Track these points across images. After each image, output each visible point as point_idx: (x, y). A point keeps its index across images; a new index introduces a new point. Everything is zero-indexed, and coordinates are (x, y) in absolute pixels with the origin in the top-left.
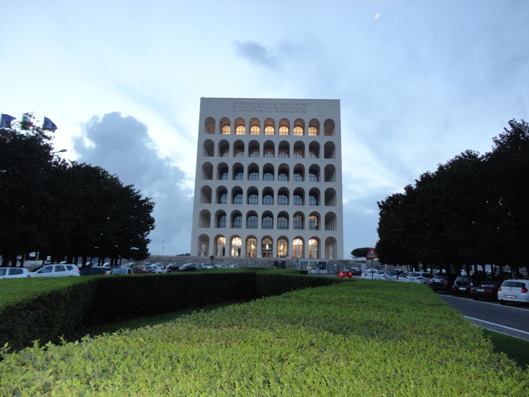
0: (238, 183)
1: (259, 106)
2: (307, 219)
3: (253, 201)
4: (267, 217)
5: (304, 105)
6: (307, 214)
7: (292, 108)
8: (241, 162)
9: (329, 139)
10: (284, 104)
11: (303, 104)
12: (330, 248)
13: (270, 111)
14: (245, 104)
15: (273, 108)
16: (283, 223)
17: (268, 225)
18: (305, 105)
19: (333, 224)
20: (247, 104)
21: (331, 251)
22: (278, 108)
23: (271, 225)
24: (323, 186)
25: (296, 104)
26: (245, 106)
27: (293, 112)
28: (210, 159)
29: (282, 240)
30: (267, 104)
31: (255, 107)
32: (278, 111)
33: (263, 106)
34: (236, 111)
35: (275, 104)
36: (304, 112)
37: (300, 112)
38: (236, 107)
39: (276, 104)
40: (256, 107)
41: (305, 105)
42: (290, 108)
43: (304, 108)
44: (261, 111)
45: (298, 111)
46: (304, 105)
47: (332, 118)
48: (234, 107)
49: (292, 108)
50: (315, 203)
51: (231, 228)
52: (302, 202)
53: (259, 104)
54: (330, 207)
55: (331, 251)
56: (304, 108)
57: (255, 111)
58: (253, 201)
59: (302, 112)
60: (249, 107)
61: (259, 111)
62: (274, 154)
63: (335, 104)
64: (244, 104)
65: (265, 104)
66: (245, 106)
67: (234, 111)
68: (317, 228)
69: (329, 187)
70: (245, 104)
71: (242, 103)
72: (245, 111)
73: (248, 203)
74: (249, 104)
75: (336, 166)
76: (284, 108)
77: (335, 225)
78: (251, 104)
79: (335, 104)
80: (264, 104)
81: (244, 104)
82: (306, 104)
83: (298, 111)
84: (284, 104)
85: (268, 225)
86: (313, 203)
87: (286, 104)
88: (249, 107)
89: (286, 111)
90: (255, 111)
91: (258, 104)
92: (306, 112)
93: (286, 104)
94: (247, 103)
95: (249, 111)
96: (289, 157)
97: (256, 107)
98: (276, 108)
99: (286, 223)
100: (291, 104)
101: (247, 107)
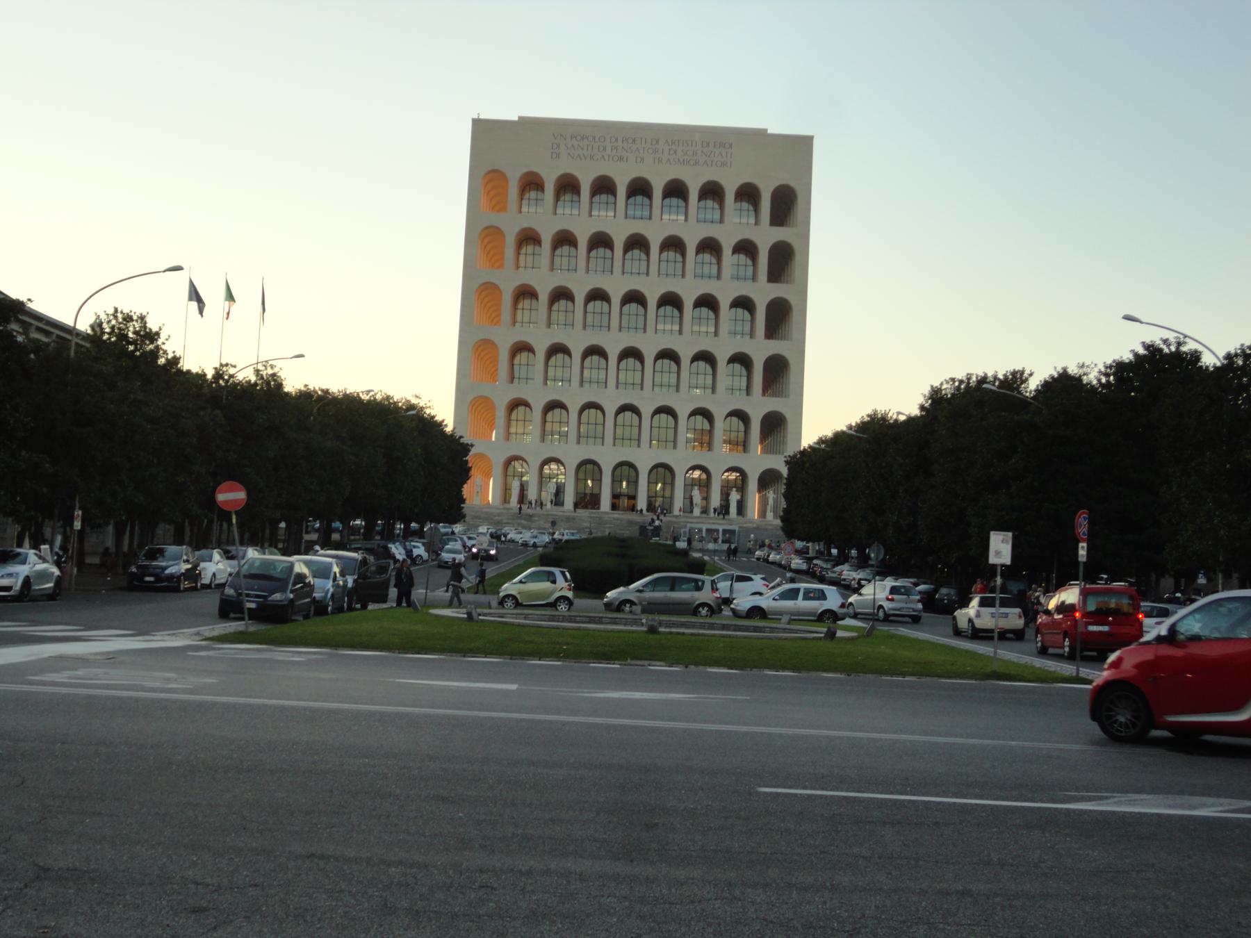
0: (560, 336)
1: (615, 144)
2: (719, 424)
3: (594, 376)
4: (626, 413)
5: (724, 147)
6: (719, 413)
7: (695, 153)
8: (569, 286)
9: (780, 234)
10: (677, 143)
11: (722, 145)
12: (768, 495)
13: (642, 160)
14: (583, 138)
15: (650, 151)
16: (663, 431)
17: (627, 435)
18: (727, 146)
19: (782, 434)
20: (585, 140)
21: (771, 502)
22: (660, 151)
23: (635, 436)
24: (760, 350)
25: (705, 145)
26: (581, 144)
27: (697, 163)
28: (496, 277)
29: (661, 470)
30: (634, 141)
31: (605, 149)
32: (660, 161)
33: (625, 145)
34: (558, 155)
35: (654, 142)
36: (724, 164)
37: (714, 163)
38: (558, 146)
39: (658, 142)
40: (609, 148)
41: (727, 146)
42: (690, 153)
43: (724, 154)
44: (621, 159)
45: (710, 163)
46: (724, 147)
47: (792, 184)
48: (555, 146)
49: (695, 153)
50: (744, 384)
51: (541, 442)
52: (711, 382)
53: (616, 140)
54: (773, 399)
55: (771, 502)
56: (724, 154)
57: (606, 158)
58: (594, 376)
59: (719, 164)
60: (590, 148)
61: (616, 158)
62: (648, 254)
63: (800, 147)
64: (579, 138)
65: (630, 141)
66: (581, 144)
67: (554, 156)
68: (745, 445)
69: (776, 352)
70: (583, 138)
71: (573, 137)
72: (583, 158)
73: (582, 382)
74: (591, 139)
75: (793, 299)
76: (675, 152)
77: (785, 440)
78: (597, 139)
79: (800, 147)
80: (627, 139)
81: (579, 138)
82: (731, 145)
83: (710, 163)
84: (677, 143)
85: (627, 435)
86: (736, 384)
87: (681, 142)
88: (590, 148)
89: (681, 160)
90: (606, 158)
91: (613, 140)
92: (729, 164)
93: (681, 142)
94: (587, 138)
95: (591, 158)
96: (683, 276)
97: (609, 148)
98: (656, 151)
99: (671, 432)
100: (694, 144)
101: (585, 148)
